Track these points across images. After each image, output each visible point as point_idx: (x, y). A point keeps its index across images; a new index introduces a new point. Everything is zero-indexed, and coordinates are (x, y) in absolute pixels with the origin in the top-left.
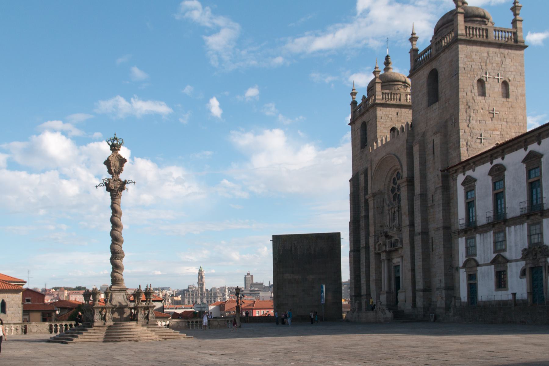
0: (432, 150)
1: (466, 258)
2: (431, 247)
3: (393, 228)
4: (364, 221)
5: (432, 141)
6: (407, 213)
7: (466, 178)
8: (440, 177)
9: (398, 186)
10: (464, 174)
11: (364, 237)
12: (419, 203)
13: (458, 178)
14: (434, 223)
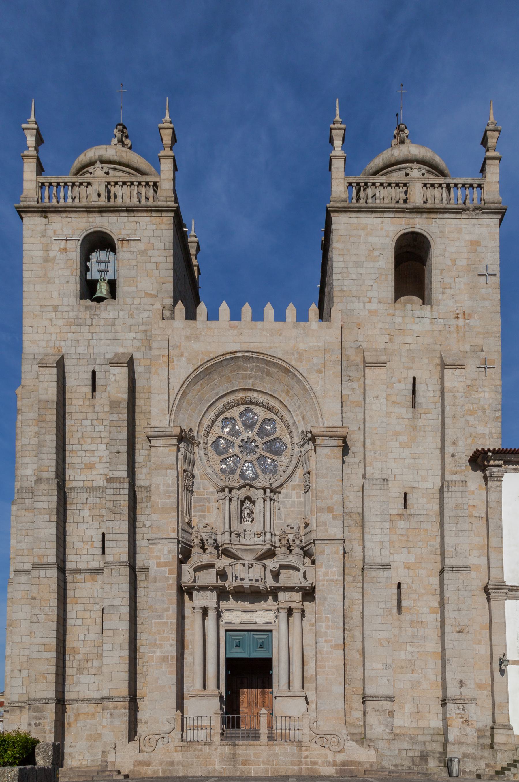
5: (411, 380)
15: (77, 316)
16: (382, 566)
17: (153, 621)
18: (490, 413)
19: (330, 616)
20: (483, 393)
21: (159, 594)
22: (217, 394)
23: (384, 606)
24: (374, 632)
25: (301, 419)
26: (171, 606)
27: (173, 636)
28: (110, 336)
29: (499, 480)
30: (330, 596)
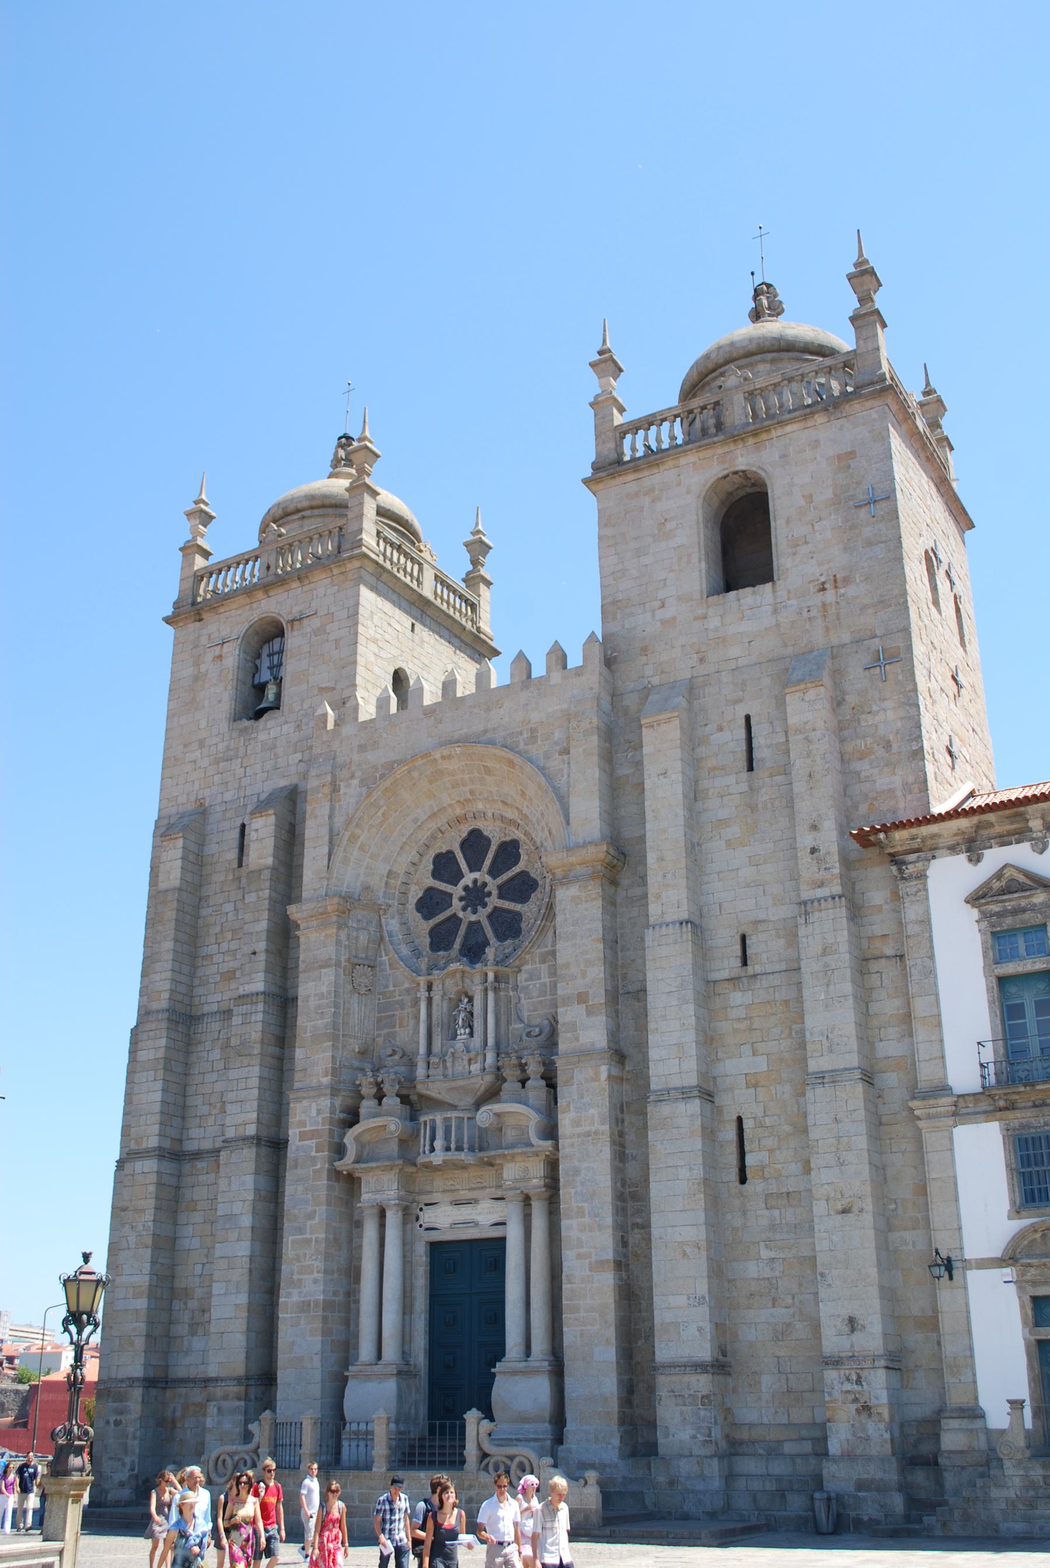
0: (742, 756)
1: (1010, 1218)
2: (733, 1159)
3: (449, 1064)
4: (260, 1017)
5: (742, 722)
6: (598, 996)
7: (999, 875)
8: (836, 857)
9: (466, 888)
10: (975, 859)
11: (256, 1092)
12: (688, 960)
13: (928, 873)
14: (754, 1055)
15: (227, 747)
16: (683, 1093)
17: (290, 1238)
18: (900, 747)
19: (585, 1205)
20: (882, 712)
21: (300, 1188)
22: (416, 820)
23: (688, 1174)
24: (669, 1230)
25: (547, 833)
26: (317, 1208)
27: (319, 1264)
28: (268, 765)
29: (922, 876)
30: (585, 1165)
